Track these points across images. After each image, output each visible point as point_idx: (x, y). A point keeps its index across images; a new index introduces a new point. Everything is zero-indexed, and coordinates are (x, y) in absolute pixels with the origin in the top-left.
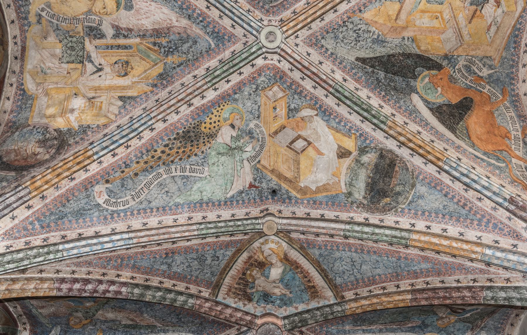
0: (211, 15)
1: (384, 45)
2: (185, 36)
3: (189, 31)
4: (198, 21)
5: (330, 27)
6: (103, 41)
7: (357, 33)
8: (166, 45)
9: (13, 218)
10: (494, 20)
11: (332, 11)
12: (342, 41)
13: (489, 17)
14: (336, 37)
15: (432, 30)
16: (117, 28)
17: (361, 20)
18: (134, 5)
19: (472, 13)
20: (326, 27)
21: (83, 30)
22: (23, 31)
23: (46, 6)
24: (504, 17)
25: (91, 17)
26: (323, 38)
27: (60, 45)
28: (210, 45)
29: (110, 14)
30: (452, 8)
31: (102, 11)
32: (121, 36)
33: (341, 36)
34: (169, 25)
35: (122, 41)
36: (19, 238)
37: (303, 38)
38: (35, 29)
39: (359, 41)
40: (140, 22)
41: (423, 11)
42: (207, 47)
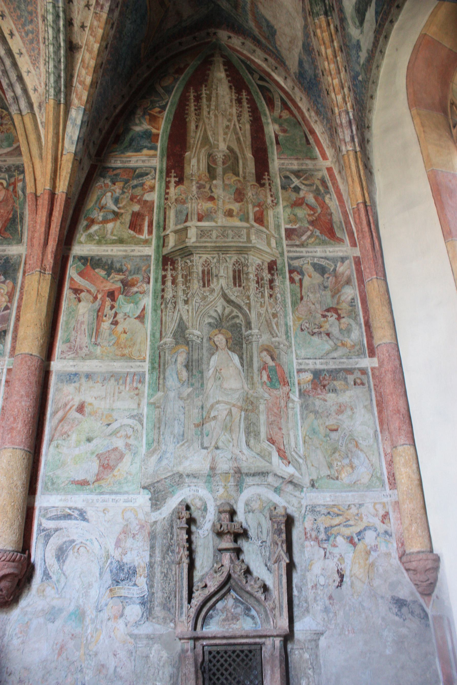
9: (21, 54)
36: (39, 50)
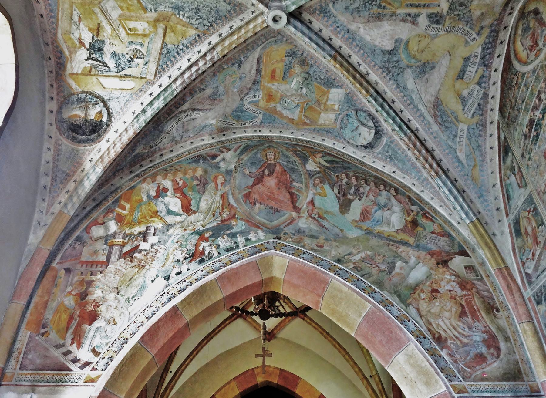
0: (329, 32)
1: (172, 5)
2: (355, 14)
3: (351, 18)
4: (341, 28)
5: (223, 21)
6: (430, 11)
7: (199, 16)
8: (374, 6)
10: (78, 26)
11: (224, 35)
12: (211, 9)
13: (84, 28)
14: (217, 12)
15: (130, 19)
16: (414, 23)
17: (197, 28)
18: (393, 44)
19: (100, 34)
20: (227, 21)
21: (445, 21)
22: (500, 20)
23: (469, 43)
24: (70, 29)
25: (434, 33)
26: (229, 11)
27: (471, 8)
28: (333, 6)
29: (416, 35)
30: (119, 38)
31: (423, 38)
32: (413, 15)
33: (213, 13)
34: (368, 24)
35: (413, 11)
37: (247, 11)
38: (487, 22)
39: (196, 8)
40: (392, 28)
41: (145, 35)
42: (336, 4)
